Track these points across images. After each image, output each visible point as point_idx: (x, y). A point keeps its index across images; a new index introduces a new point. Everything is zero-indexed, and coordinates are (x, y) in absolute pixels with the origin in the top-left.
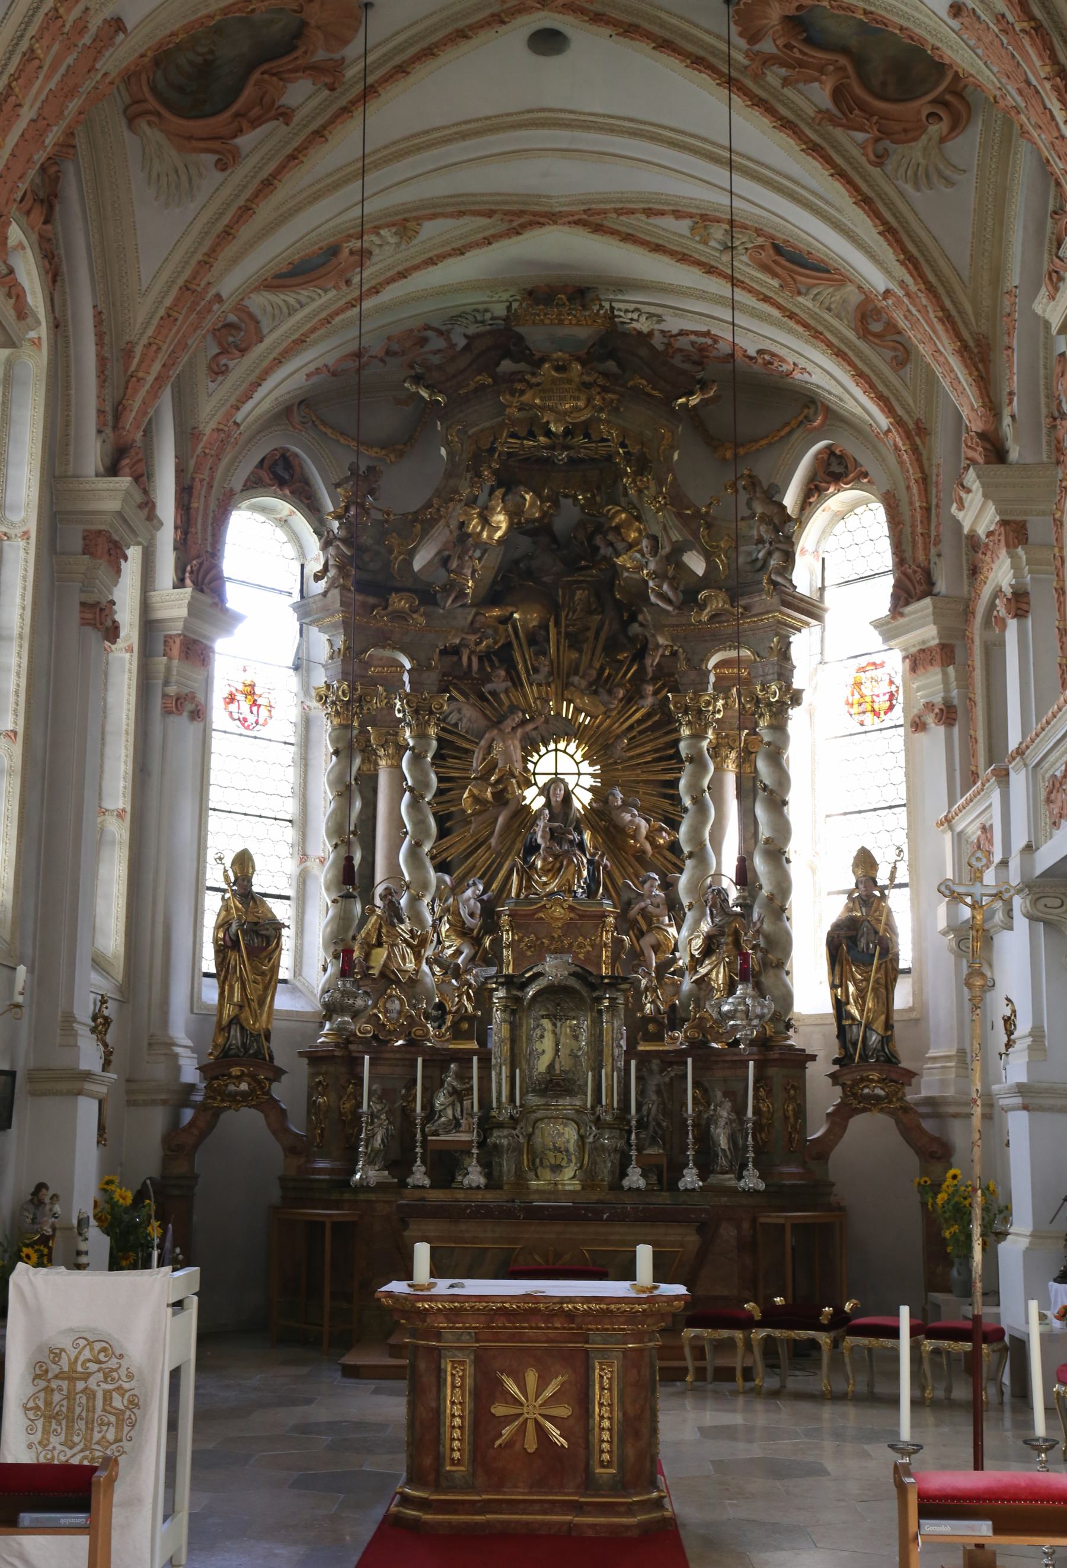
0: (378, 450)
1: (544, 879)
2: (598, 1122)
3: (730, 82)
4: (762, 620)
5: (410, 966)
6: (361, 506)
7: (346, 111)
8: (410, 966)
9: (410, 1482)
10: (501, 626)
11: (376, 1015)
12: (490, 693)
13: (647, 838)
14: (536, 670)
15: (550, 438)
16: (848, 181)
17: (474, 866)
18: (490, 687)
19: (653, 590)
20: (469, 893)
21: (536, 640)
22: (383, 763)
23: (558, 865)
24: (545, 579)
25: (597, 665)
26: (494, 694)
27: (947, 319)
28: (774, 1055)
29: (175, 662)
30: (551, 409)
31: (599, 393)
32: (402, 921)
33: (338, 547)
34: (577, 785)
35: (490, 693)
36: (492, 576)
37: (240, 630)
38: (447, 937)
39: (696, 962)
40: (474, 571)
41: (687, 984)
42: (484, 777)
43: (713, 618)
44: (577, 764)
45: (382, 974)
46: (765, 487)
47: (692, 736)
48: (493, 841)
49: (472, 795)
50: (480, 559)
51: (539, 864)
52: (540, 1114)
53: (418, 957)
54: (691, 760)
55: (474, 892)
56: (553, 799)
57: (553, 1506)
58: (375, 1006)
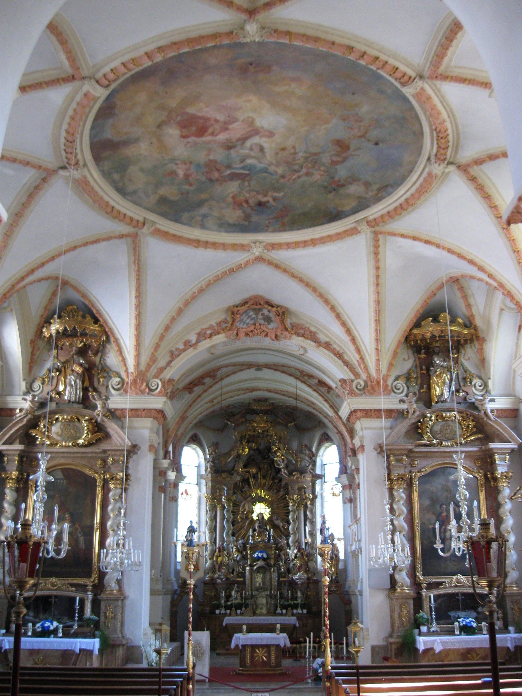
2: (271, 597)
3: (297, 378)
6: (215, 452)
7: (217, 382)
9: (240, 667)
16: (323, 397)
18: (244, 489)
20: (240, 542)
21: (255, 477)
22: (218, 509)
26: (245, 491)
28: (311, 581)
29: (172, 489)
30: (258, 427)
37: (186, 479)
39: (293, 560)
41: (291, 565)
42: (243, 512)
43: (296, 478)
45: (221, 564)
48: (245, 528)
49: (240, 517)
52: (258, 596)
54: (292, 511)
57: (264, 670)
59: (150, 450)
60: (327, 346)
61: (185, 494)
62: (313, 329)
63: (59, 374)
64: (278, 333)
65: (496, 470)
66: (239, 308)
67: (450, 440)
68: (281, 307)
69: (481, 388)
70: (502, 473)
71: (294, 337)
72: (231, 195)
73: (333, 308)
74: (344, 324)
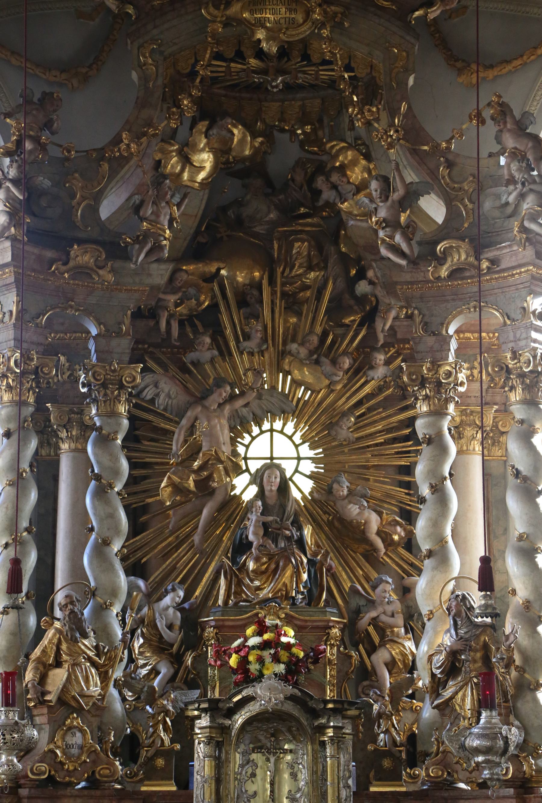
0: (58, 74)
1: (257, 583)
4: (513, 275)
5: (95, 690)
6: (36, 140)
8: (95, 690)
10: (205, 284)
11: (52, 752)
12: (193, 363)
13: (378, 533)
14: (247, 337)
15: (261, 60)
17: (174, 568)
19: (383, 241)
20: (167, 600)
22: (64, 446)
23: (273, 566)
24: (258, 229)
25: (319, 330)
26: (197, 364)
31: (320, 5)
32: (85, 636)
33: (8, 189)
34: (296, 471)
35: (193, 363)
36: (196, 224)
38: (141, 653)
40: (171, 221)
43: (454, 274)
44: (297, 446)
45: (61, 701)
46: (517, 114)
47: (430, 413)
48: (196, 538)
49: (171, 484)
50: (179, 205)
51: (251, 565)
53: (104, 677)
54: (429, 441)
55: (173, 599)
56: (267, 488)
58: (52, 740)
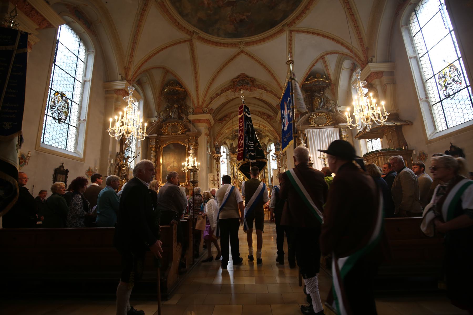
3: (259, 116)
7: (231, 120)
27: (277, 132)
46: (264, 143)
59: (205, 135)
60: (271, 92)
61: (222, 162)
62: (265, 86)
63: (169, 109)
64: (252, 88)
65: (342, 134)
66: (236, 80)
67: (322, 124)
68: (252, 78)
69: (333, 104)
70: (344, 135)
71: (258, 89)
72: (229, 16)
73: (272, 75)
74: (277, 81)
